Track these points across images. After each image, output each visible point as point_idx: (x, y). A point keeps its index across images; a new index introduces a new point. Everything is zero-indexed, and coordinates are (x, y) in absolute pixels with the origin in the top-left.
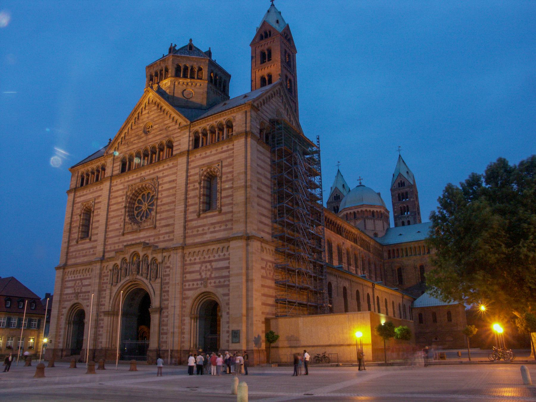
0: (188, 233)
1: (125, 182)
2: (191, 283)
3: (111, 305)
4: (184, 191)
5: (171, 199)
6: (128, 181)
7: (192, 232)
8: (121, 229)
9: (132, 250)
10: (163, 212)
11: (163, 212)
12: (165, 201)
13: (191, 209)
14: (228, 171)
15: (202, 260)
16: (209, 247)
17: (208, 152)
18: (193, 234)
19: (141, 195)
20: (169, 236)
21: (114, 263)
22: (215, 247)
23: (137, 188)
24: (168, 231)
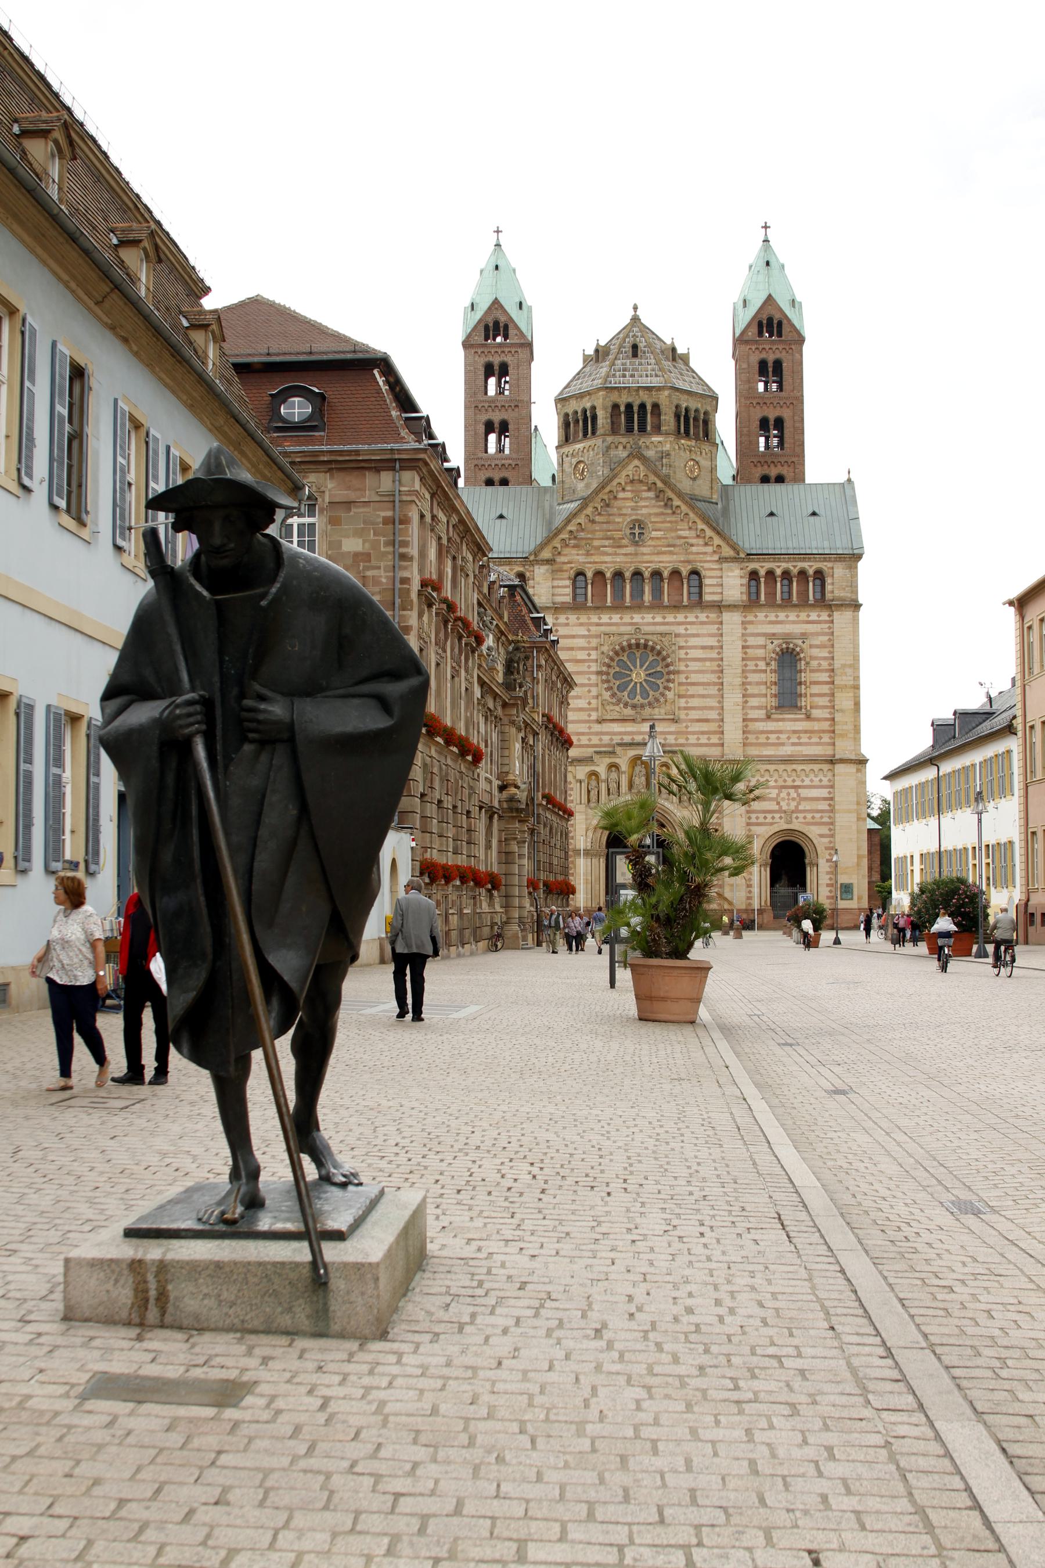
0: (747, 738)
1: (591, 624)
2: (761, 816)
3: (589, 840)
4: (739, 671)
5: (713, 678)
6: (598, 625)
7: (757, 738)
8: (592, 710)
9: (632, 753)
10: (692, 696)
11: (692, 696)
12: (694, 678)
13: (754, 702)
14: (820, 655)
15: (781, 783)
16: (794, 766)
17: (782, 615)
18: (760, 741)
19: (626, 654)
20: (709, 739)
21: (588, 769)
22: (807, 767)
23: (625, 643)
24: (706, 729)
